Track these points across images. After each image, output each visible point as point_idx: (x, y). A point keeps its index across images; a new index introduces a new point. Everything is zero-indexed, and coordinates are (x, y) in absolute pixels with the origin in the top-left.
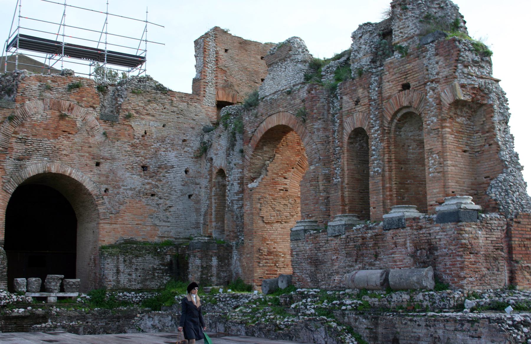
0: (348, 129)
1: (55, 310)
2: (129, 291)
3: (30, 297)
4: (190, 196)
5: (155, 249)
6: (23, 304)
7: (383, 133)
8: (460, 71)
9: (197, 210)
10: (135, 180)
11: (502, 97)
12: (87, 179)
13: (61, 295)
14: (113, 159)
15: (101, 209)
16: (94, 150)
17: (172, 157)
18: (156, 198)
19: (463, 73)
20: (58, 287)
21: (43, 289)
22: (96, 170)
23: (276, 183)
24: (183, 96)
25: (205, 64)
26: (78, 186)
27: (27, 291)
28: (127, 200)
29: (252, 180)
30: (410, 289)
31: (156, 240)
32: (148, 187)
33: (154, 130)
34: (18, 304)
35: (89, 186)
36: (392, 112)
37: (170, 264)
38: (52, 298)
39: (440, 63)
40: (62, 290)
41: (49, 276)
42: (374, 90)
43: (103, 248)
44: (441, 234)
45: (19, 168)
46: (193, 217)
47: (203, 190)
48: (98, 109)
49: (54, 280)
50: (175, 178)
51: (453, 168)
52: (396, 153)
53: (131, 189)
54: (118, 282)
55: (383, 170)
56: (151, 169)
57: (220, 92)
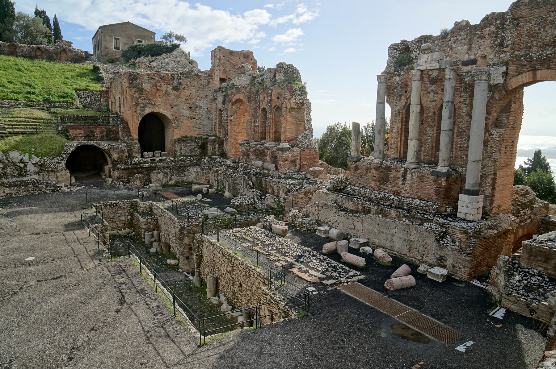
0: (261, 107)
2: (186, 156)
3: (149, 160)
5: (195, 140)
9: (212, 124)
10: (188, 113)
12: (168, 114)
13: (161, 158)
14: (178, 105)
16: (170, 102)
17: (201, 103)
20: (159, 155)
21: (154, 156)
22: (171, 110)
23: (240, 118)
25: (215, 62)
26: (165, 116)
29: (231, 116)
30: (269, 170)
31: (196, 136)
34: (145, 163)
35: (169, 117)
37: (201, 146)
38: (157, 159)
40: (161, 156)
43: (175, 140)
44: (279, 154)
45: (142, 111)
46: (210, 127)
47: (214, 115)
49: (157, 152)
50: (203, 111)
57: (221, 75)
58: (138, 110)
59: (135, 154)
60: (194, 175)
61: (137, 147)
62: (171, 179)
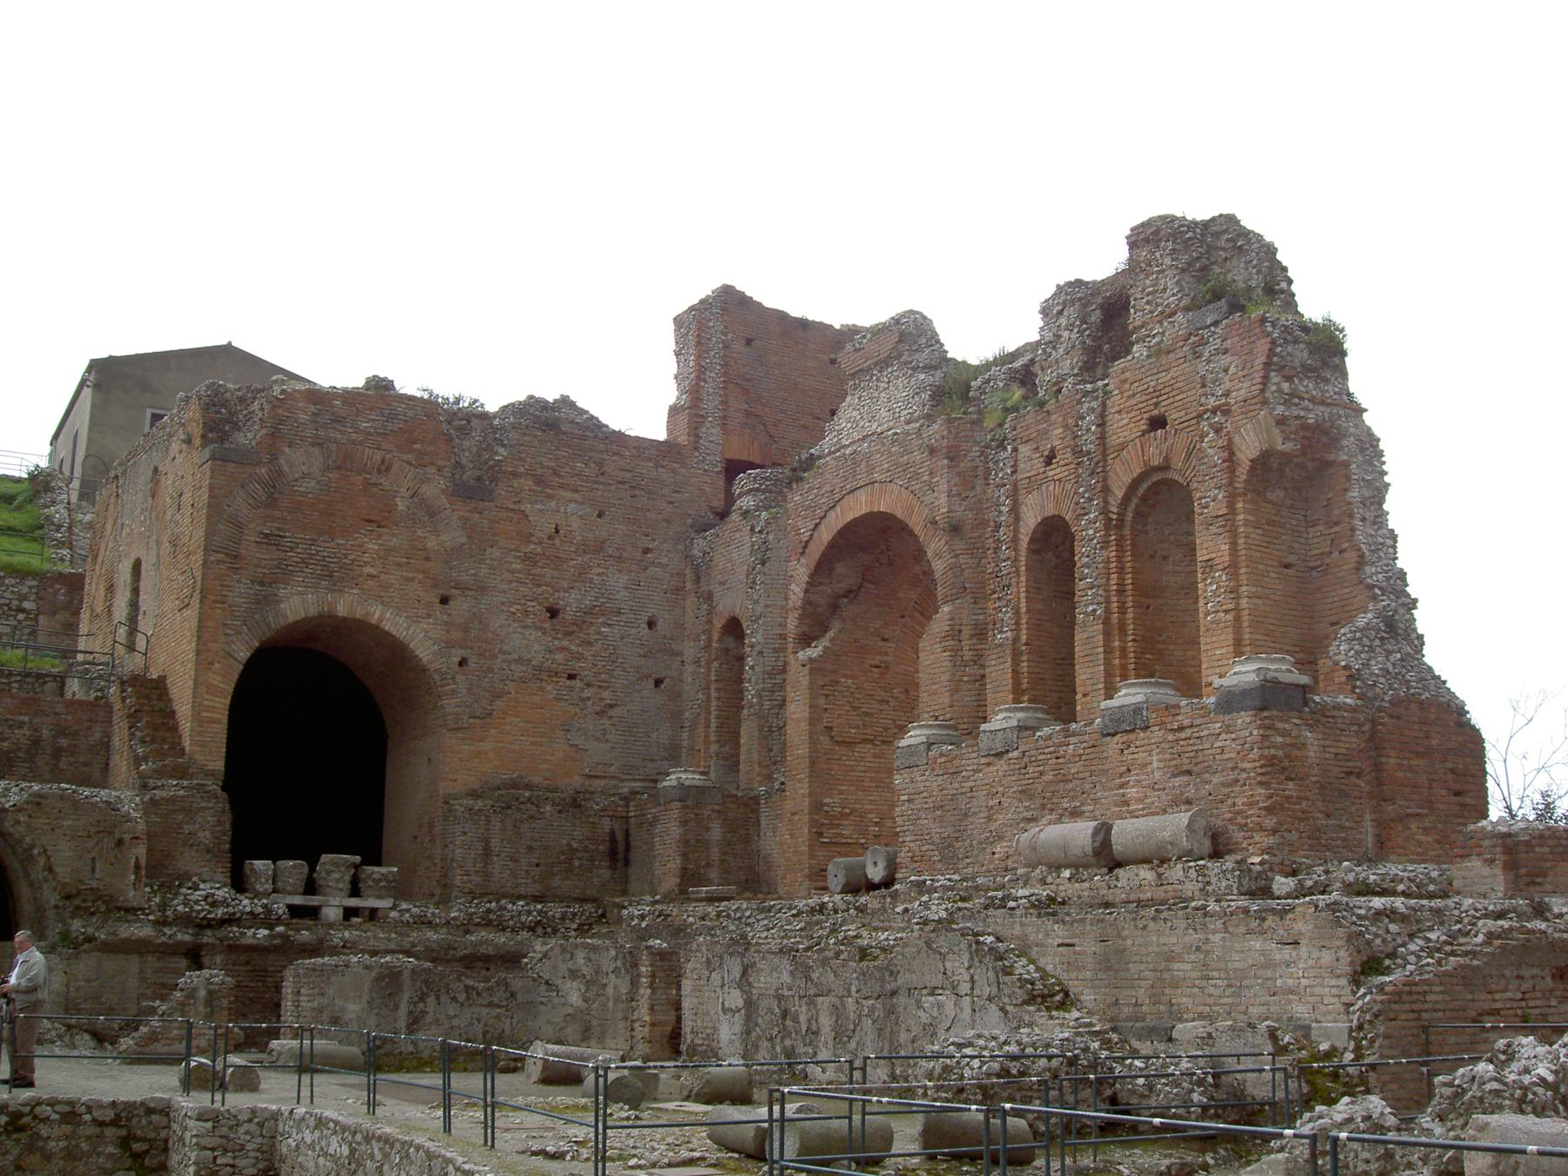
1: (337, 936)
4: (658, 683)
6: (268, 920)
7: (1107, 527)
8: (1274, 388)
10: (532, 643)
11: (1370, 447)
12: (420, 636)
13: (353, 902)
14: (482, 589)
15: (450, 705)
18: (577, 683)
19: (1280, 391)
20: (345, 885)
21: (311, 887)
24: (642, 446)
25: (701, 373)
26: (397, 653)
27: (275, 891)
28: (511, 686)
32: (559, 657)
33: (576, 524)
34: (254, 919)
36: (1128, 480)
39: (1232, 370)
40: (355, 892)
41: (325, 858)
42: (1088, 430)
45: (265, 601)
48: (447, 472)
49: (335, 866)
51: (1259, 602)
52: (1135, 572)
53: (520, 661)
54: (487, 875)
55: (1108, 611)
56: (569, 614)
58: (240, 592)
59: (188, 861)
60: (575, 999)
61: (210, 821)
62: (415, 1022)
